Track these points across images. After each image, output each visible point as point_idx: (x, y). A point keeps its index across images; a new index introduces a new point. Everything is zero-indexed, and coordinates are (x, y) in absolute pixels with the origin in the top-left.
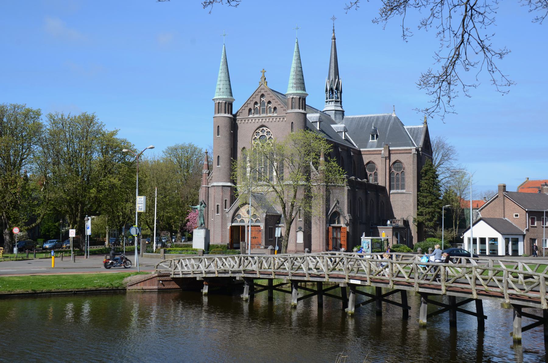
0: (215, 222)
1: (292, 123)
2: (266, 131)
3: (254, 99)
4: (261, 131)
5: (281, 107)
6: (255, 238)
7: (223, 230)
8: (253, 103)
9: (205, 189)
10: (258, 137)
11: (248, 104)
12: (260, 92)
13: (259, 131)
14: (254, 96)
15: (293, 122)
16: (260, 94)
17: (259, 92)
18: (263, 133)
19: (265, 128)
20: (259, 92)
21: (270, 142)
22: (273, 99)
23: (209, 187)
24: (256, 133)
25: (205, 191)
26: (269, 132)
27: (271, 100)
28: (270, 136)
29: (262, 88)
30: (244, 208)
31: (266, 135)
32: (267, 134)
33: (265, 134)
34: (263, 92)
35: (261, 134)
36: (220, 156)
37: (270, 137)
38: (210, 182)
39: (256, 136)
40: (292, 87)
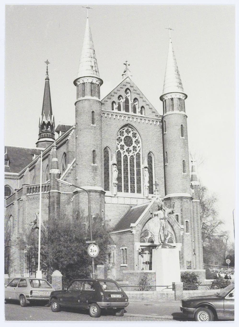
1: (182, 125)
2: (132, 132)
3: (118, 92)
5: (150, 108)
8: (117, 96)
10: (123, 138)
11: (111, 96)
12: (126, 85)
13: (123, 130)
14: (119, 88)
15: (183, 125)
16: (125, 88)
17: (124, 85)
18: (128, 134)
19: (130, 129)
20: (124, 85)
21: (136, 145)
22: (141, 97)
26: (135, 134)
27: (137, 97)
28: (137, 138)
29: (128, 82)
31: (131, 136)
33: (130, 135)
34: (128, 86)
35: (125, 134)
37: (137, 140)
40: (178, 86)
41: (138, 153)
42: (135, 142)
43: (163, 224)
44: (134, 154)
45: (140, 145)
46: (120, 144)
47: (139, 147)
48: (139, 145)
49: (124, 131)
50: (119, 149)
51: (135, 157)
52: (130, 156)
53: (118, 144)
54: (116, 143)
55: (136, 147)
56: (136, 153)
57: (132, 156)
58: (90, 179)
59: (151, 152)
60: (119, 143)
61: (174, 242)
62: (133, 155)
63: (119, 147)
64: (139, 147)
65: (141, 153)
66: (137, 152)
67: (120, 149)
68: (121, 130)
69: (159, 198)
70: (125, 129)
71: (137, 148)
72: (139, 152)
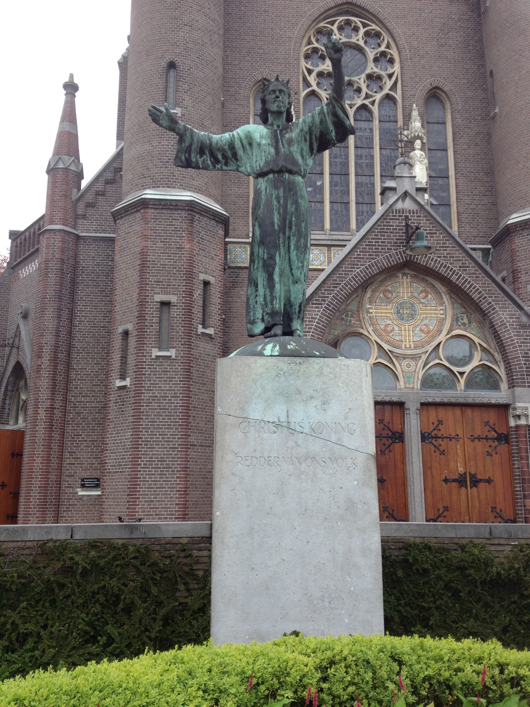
0: (146, 396)
4: (341, 28)
6: (475, 482)
7: (192, 439)
9: (63, 241)
23: (78, 237)
24: (319, 32)
25: (63, 251)
28: (383, 48)
30: (388, 300)
31: (361, 43)
32: (366, 42)
33: (359, 39)
36: (178, 61)
37: (383, 54)
38: (84, 217)
39: (316, 45)
41: (388, 97)
42: (376, 60)
43: (269, 203)
44: (371, 100)
45: (397, 67)
46: (317, 70)
47: (390, 76)
48: (390, 71)
49: (335, 28)
50: (311, 86)
51: (375, 109)
52: (354, 108)
53: (310, 72)
54: (298, 64)
55: (379, 78)
56: (378, 97)
57: (363, 107)
58: (150, 165)
59: (436, 88)
60: (311, 68)
61: (504, 386)
62: (366, 102)
63: (312, 79)
64: (390, 76)
65: (398, 96)
66: (386, 91)
67: (315, 87)
68: (322, 24)
69: (413, 192)
70: (336, 20)
71: (386, 79)
72: (391, 93)
